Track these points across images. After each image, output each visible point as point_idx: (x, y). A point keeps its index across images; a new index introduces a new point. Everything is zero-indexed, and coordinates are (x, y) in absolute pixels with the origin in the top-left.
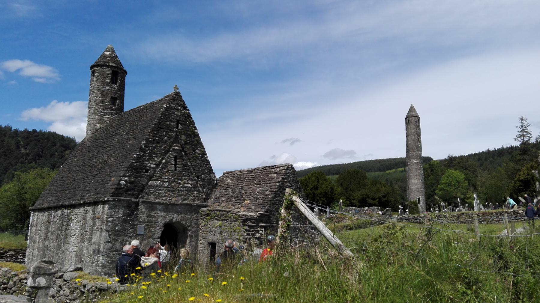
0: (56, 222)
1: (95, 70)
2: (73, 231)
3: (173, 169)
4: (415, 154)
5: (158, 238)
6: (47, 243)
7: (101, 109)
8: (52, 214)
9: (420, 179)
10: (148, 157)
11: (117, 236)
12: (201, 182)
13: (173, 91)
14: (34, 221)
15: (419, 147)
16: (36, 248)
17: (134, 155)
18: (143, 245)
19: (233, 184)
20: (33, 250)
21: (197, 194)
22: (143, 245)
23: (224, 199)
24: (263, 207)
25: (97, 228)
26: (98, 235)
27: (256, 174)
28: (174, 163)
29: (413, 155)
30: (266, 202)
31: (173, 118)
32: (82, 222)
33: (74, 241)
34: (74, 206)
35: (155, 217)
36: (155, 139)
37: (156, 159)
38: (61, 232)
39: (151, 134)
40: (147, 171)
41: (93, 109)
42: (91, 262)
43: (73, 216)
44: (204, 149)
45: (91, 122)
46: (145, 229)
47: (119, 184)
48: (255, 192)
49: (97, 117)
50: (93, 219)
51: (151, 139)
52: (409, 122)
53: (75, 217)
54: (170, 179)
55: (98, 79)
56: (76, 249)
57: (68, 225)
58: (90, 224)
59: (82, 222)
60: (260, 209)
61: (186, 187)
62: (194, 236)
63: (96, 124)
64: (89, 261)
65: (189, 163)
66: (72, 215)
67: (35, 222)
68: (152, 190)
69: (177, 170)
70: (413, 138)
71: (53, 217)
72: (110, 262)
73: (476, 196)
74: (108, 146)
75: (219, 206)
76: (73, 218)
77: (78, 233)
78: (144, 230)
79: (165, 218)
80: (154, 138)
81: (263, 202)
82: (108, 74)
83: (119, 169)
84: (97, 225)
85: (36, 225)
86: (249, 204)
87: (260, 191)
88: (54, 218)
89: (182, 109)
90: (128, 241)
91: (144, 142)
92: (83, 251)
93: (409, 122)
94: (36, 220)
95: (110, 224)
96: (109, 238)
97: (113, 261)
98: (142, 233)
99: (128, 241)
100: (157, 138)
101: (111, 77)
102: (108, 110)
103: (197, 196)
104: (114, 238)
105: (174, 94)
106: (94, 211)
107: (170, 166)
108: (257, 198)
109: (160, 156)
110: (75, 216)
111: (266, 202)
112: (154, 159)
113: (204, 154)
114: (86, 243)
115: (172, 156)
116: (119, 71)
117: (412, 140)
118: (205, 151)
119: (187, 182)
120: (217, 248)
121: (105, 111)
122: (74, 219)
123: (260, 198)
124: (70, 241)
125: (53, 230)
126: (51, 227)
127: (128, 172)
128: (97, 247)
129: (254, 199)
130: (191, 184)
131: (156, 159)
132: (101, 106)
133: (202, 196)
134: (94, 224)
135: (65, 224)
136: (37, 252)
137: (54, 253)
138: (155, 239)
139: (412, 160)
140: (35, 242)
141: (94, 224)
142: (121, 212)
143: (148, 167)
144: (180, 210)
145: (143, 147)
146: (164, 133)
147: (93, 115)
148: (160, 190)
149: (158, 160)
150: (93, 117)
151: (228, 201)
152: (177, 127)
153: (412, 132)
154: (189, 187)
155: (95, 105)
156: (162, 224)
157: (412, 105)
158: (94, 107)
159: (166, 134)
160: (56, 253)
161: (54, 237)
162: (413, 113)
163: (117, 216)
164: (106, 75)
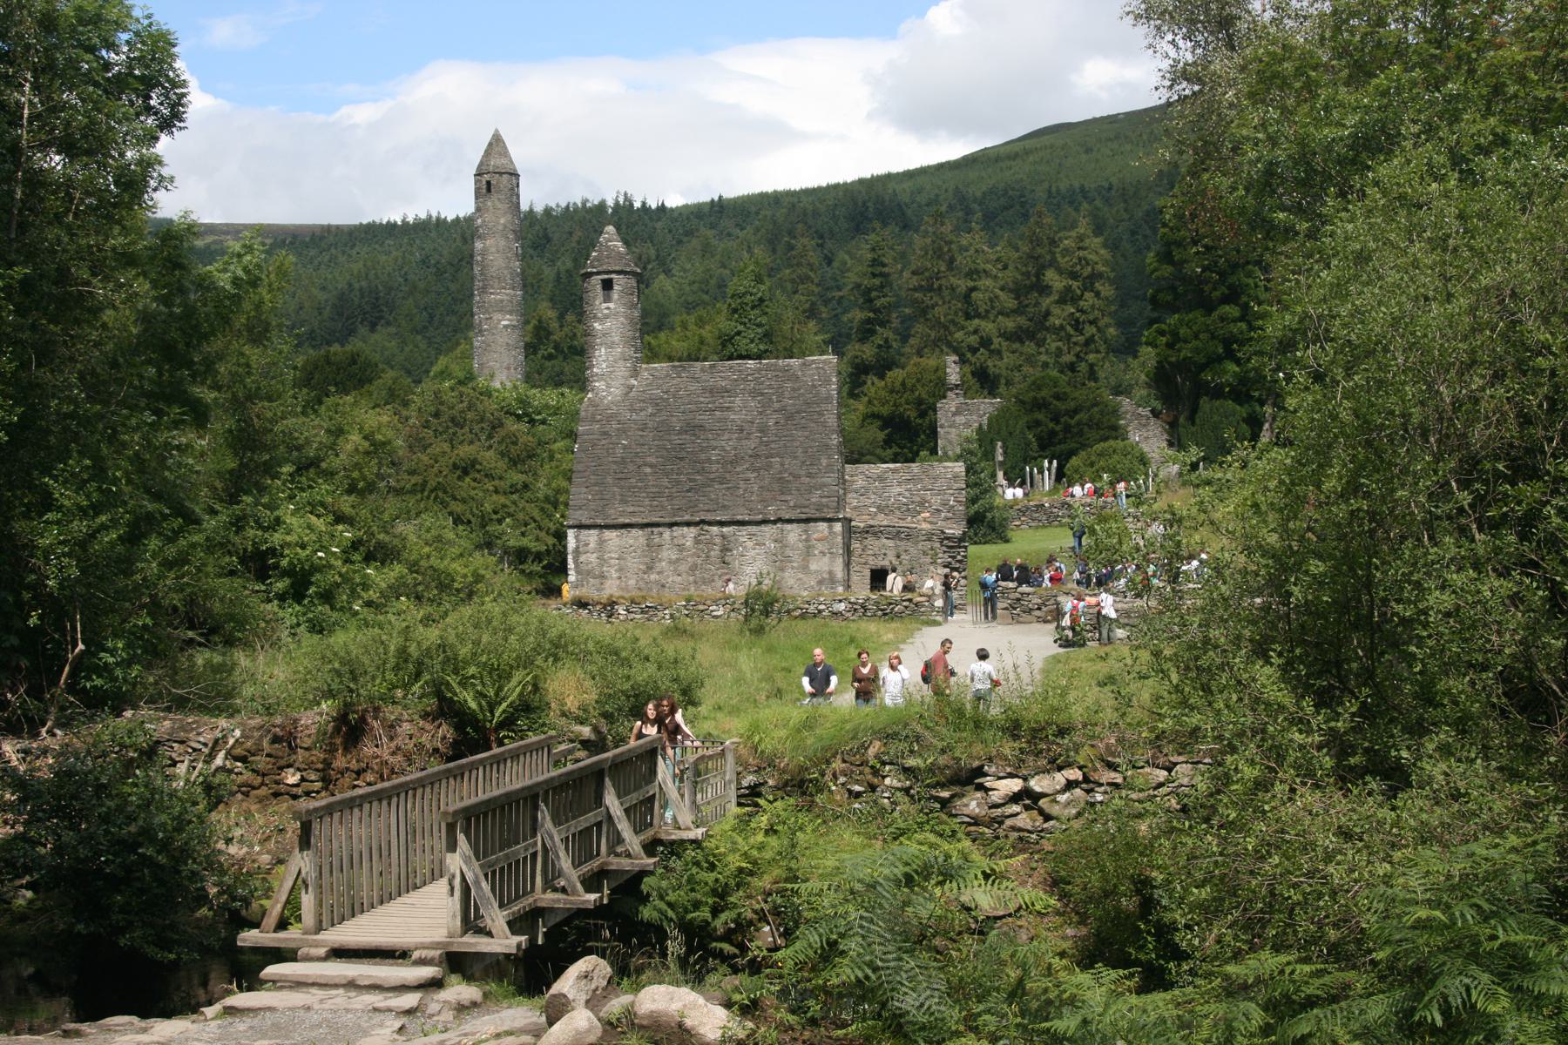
4: (505, 297)
29: (502, 301)
52: (489, 190)
70: (503, 243)
93: (489, 190)
139: (497, 316)
147: (621, 362)
157: (497, 131)
161: (683, 567)
162: (504, 161)
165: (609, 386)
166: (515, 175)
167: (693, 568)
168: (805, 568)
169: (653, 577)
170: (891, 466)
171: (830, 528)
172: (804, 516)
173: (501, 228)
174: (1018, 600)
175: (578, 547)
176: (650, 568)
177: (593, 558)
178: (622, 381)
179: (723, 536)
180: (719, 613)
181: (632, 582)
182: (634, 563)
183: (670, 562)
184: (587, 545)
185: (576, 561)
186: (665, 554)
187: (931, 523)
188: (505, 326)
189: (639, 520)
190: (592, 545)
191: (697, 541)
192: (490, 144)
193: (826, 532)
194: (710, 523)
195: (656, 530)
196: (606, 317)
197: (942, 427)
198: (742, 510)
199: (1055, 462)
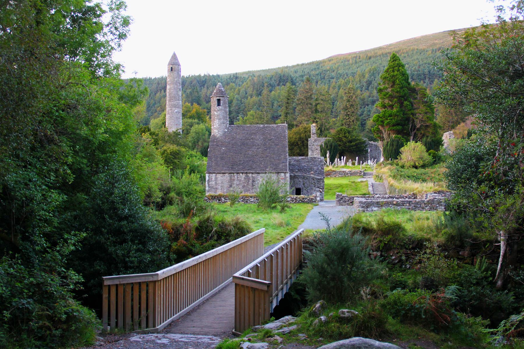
29: (175, 104)
70: (176, 86)
93: (172, 70)
161: (241, 186)
162: (177, 61)
165: (219, 131)
166: (179, 65)
167: (244, 187)
169: (231, 189)
170: (302, 157)
171: (285, 175)
172: (277, 172)
173: (175, 82)
174: (342, 198)
176: (231, 186)
177: (214, 183)
178: (223, 130)
179: (252, 177)
180: (252, 200)
181: (225, 190)
182: (226, 185)
183: (237, 185)
184: (212, 179)
185: (208, 184)
186: (235, 182)
187: (314, 175)
188: (176, 112)
189: (228, 172)
190: (213, 179)
191: (245, 178)
192: (172, 57)
193: (284, 177)
194: (249, 173)
195: (232, 175)
196: (218, 110)
197: (310, 146)
198: (259, 170)
199: (345, 157)
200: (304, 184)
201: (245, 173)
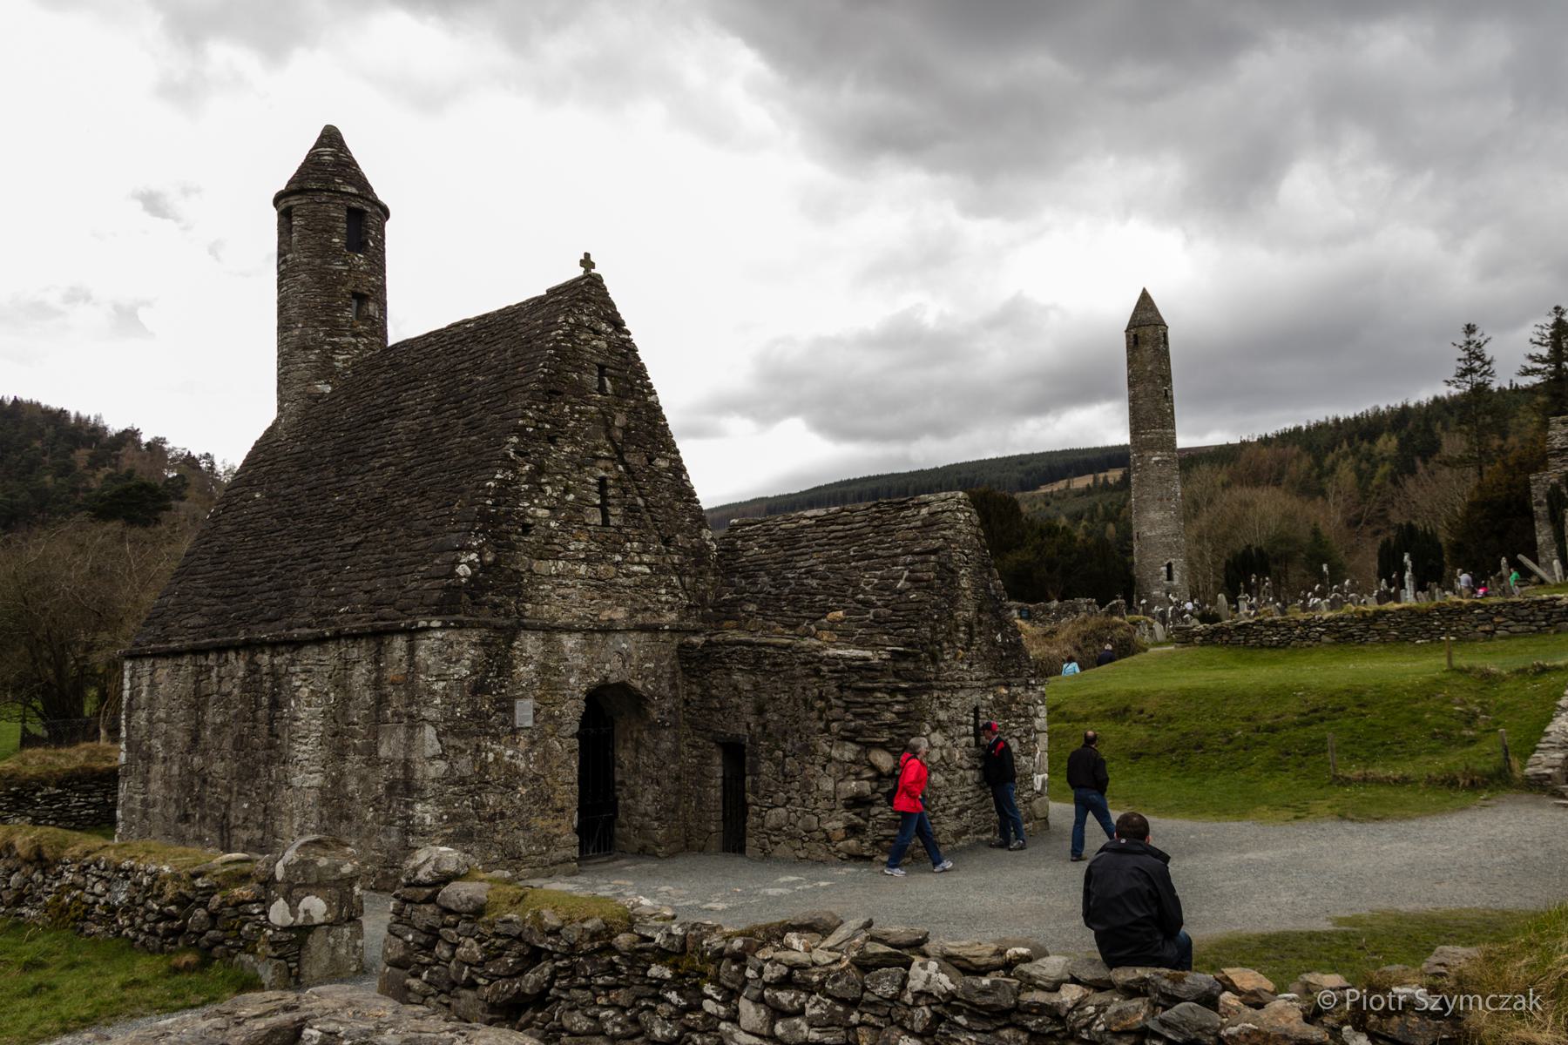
0: (230, 693)
1: (290, 208)
2: (299, 723)
3: (598, 520)
5: (572, 737)
6: (197, 761)
7: (321, 334)
8: (209, 669)
9: (1171, 509)
10: (526, 487)
11: (461, 734)
12: (676, 557)
13: (580, 272)
14: (140, 692)
15: (1168, 415)
16: (158, 777)
17: (488, 480)
18: (532, 759)
19: (775, 558)
20: (146, 782)
21: (667, 593)
22: (532, 759)
23: (752, 607)
24: (895, 629)
25: (394, 714)
26: (402, 736)
27: (847, 527)
28: (598, 502)
29: (1152, 439)
30: (902, 613)
31: (589, 361)
32: (332, 695)
33: (306, 756)
34: (297, 645)
35: (560, 671)
36: (544, 428)
37: (549, 489)
38: (255, 727)
39: (531, 414)
40: (527, 529)
41: (296, 332)
42: (382, 819)
43: (294, 678)
44: (677, 452)
45: (295, 374)
46: (537, 711)
47: (452, 574)
48: (859, 584)
49: (313, 357)
50: (377, 684)
51: (531, 429)
53: (305, 680)
54: (590, 551)
55: (303, 238)
56: (317, 780)
57: (276, 704)
58: (365, 702)
59: (332, 695)
60: (886, 637)
61: (635, 574)
62: (668, 724)
63: (310, 379)
64: (374, 818)
65: (640, 501)
66: (294, 674)
67: (143, 695)
68: (543, 590)
69: (611, 524)
70: (1150, 388)
71: (215, 680)
72: (445, 817)
73: (1411, 558)
74: (376, 452)
75: (738, 628)
76: (298, 683)
77: (321, 728)
78: (535, 715)
79: (585, 673)
80: (540, 425)
81: (891, 615)
82: (334, 219)
83: (442, 525)
84: (395, 704)
85: (151, 700)
86: (842, 621)
87: (876, 581)
88: (219, 682)
89: (609, 330)
90: (492, 750)
91: (515, 440)
92: (345, 786)
93: (1136, 343)
94: (145, 689)
95: (438, 701)
96: (438, 746)
97: (455, 815)
98: (529, 723)
99: (492, 750)
100: (547, 426)
101: (348, 229)
102: (346, 336)
103: (667, 602)
104: (451, 743)
105: (587, 284)
106: (377, 662)
107: (589, 510)
108: (868, 604)
109: (561, 480)
110: (303, 676)
111: (902, 613)
112: (544, 491)
113: (678, 469)
114: (354, 761)
115: (592, 480)
116: (369, 210)
117: (1146, 396)
118: (680, 460)
119: (637, 559)
120: (748, 758)
121: (336, 339)
122: (300, 686)
123: (879, 603)
124: (294, 753)
125: (218, 721)
126: (210, 712)
127: (476, 535)
128: (399, 773)
129: (860, 606)
130: (649, 565)
131: (549, 489)
132: (322, 322)
133: (680, 599)
134: (381, 701)
135: (265, 701)
136: (162, 791)
137: (230, 792)
138: (564, 738)
139: (1148, 454)
140: (149, 757)
141: (381, 701)
142: (467, 662)
143: (531, 517)
144: (625, 645)
145: (512, 454)
146: (567, 409)
147: (299, 353)
148: (566, 586)
149: (555, 495)
150: (299, 360)
151: (769, 613)
152: (602, 389)
153: (1146, 370)
154: (645, 574)
155: (302, 319)
156: (581, 691)
157: (1144, 289)
158: (300, 325)
159: (573, 412)
160: (239, 793)
161: (227, 744)
162: (1149, 315)
163: (456, 677)
164: (331, 223)
166: (1162, 323)
168: (371, 753)
171: (411, 650)
173: (1148, 374)
175: (131, 698)
194: (261, 645)
200: (760, 711)
201: (237, 648)
